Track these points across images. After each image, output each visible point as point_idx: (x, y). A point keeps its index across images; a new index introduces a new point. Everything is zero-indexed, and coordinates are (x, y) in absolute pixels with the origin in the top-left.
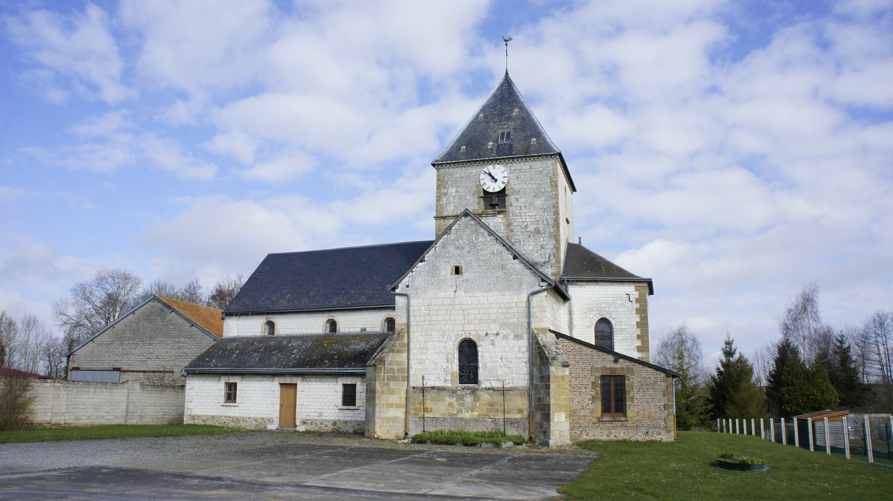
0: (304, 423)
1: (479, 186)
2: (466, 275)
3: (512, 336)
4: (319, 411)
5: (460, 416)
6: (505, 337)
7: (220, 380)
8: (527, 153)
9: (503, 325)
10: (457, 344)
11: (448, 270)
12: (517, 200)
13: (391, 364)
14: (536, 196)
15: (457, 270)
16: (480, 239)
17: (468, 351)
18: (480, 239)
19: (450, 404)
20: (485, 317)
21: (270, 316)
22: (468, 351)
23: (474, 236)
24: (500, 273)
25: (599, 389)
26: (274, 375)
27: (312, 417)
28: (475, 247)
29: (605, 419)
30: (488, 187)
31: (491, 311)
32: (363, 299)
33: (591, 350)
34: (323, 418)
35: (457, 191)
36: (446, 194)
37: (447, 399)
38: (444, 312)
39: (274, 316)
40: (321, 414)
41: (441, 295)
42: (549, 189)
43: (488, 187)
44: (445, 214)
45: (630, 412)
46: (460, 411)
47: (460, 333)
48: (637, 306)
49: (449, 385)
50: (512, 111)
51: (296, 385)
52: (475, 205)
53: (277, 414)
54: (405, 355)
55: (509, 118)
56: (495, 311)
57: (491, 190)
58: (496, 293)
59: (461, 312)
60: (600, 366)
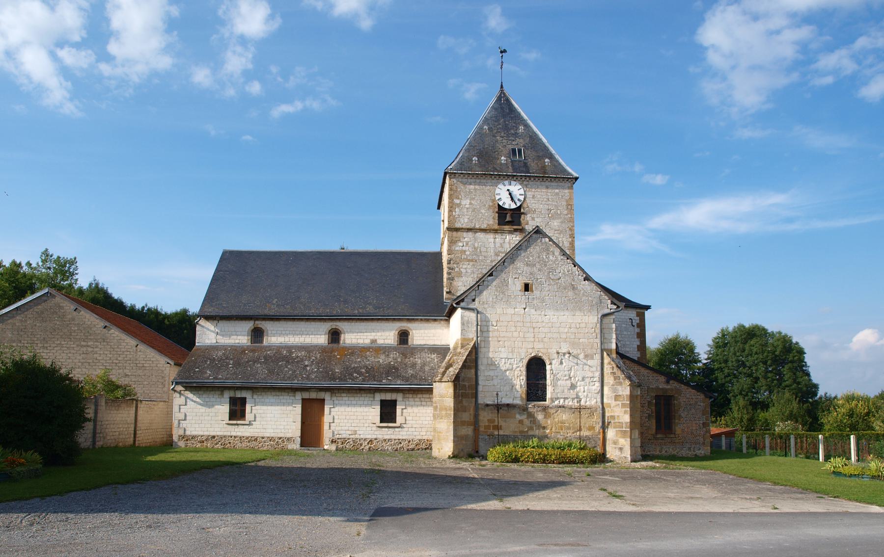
0: (332, 442)
1: (494, 200)
2: (536, 293)
3: (581, 356)
4: (353, 429)
5: (531, 433)
6: (576, 357)
7: (222, 394)
8: (545, 173)
9: (573, 344)
10: (525, 361)
11: (519, 286)
12: (533, 219)
13: (463, 380)
14: (553, 218)
15: (527, 287)
16: (551, 257)
17: (536, 368)
18: (551, 257)
19: (521, 422)
20: (555, 335)
21: (257, 322)
22: (536, 368)
23: (545, 254)
24: (570, 294)
25: (653, 408)
26: (294, 390)
27: (344, 436)
28: (546, 265)
29: (659, 436)
30: (504, 203)
31: (561, 330)
32: (370, 309)
33: (647, 371)
34: (357, 436)
35: (471, 204)
36: (459, 205)
37: (518, 416)
38: (513, 329)
39: (263, 322)
40: (355, 432)
41: (510, 311)
42: (566, 212)
43: (504, 203)
44: (458, 225)
45: (678, 429)
46: (531, 428)
47: (530, 351)
48: (637, 330)
49: (518, 402)
50: (517, 129)
51: (324, 400)
52: (489, 219)
53: (299, 433)
54: (473, 371)
55: (516, 135)
56: (566, 330)
57: (507, 206)
58: (567, 313)
59: (531, 330)
60: (654, 387)
